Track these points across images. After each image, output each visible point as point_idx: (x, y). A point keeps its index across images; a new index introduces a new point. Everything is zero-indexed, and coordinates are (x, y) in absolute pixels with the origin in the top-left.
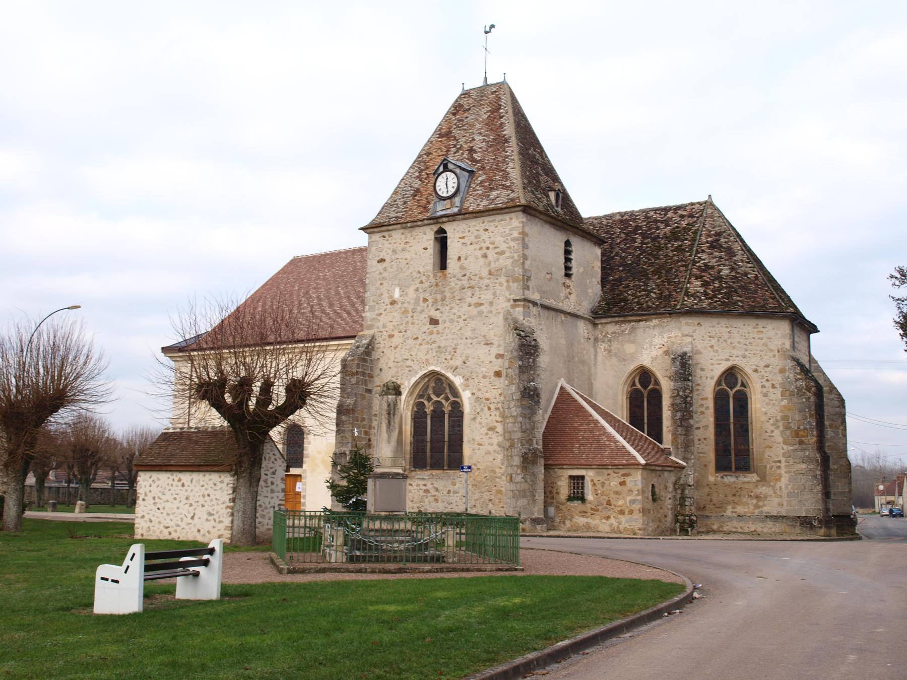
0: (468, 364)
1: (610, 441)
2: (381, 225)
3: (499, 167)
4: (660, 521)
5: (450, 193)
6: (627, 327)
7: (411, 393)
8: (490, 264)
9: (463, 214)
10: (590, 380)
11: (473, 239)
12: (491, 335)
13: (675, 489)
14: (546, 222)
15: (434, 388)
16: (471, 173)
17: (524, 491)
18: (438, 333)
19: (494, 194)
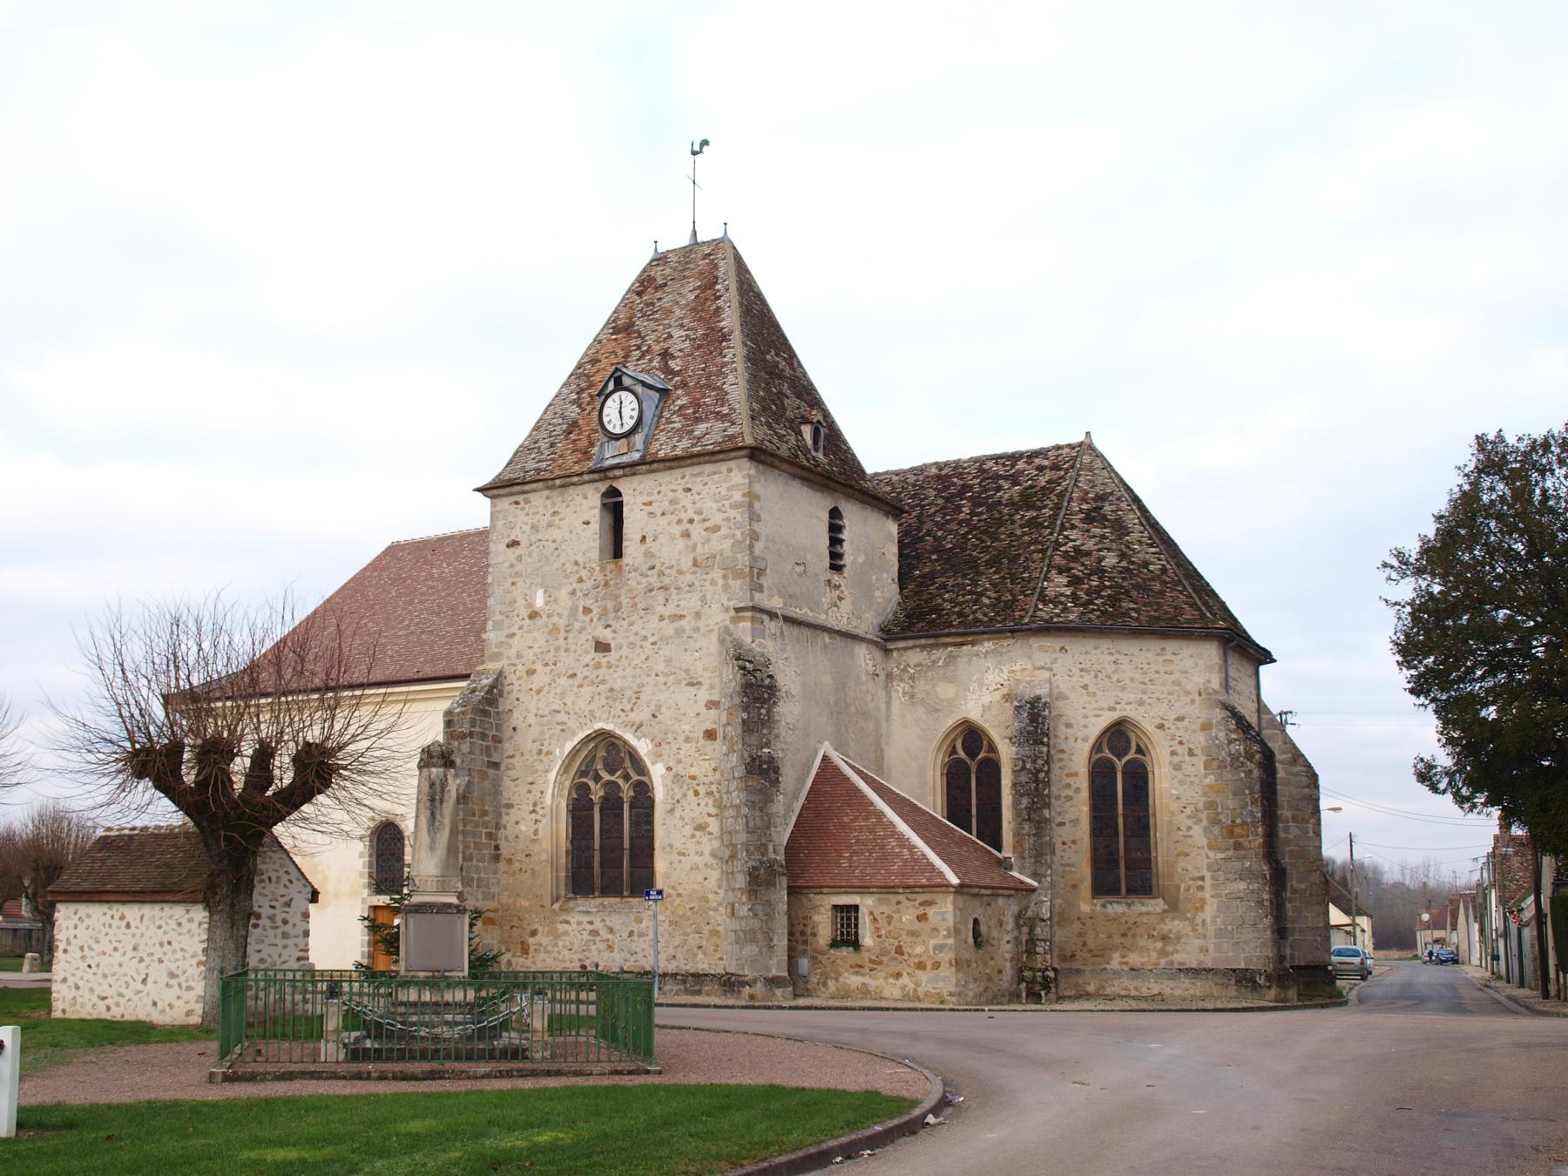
0: (660, 717)
1: (902, 846)
2: (511, 483)
3: (711, 383)
4: (990, 980)
5: (626, 428)
6: (941, 654)
7: (566, 768)
8: (694, 547)
9: (649, 463)
10: (878, 743)
11: (666, 505)
12: (698, 669)
13: (1018, 927)
14: (794, 476)
15: (605, 759)
16: (664, 393)
17: (753, 931)
18: (609, 666)
19: (702, 427)
